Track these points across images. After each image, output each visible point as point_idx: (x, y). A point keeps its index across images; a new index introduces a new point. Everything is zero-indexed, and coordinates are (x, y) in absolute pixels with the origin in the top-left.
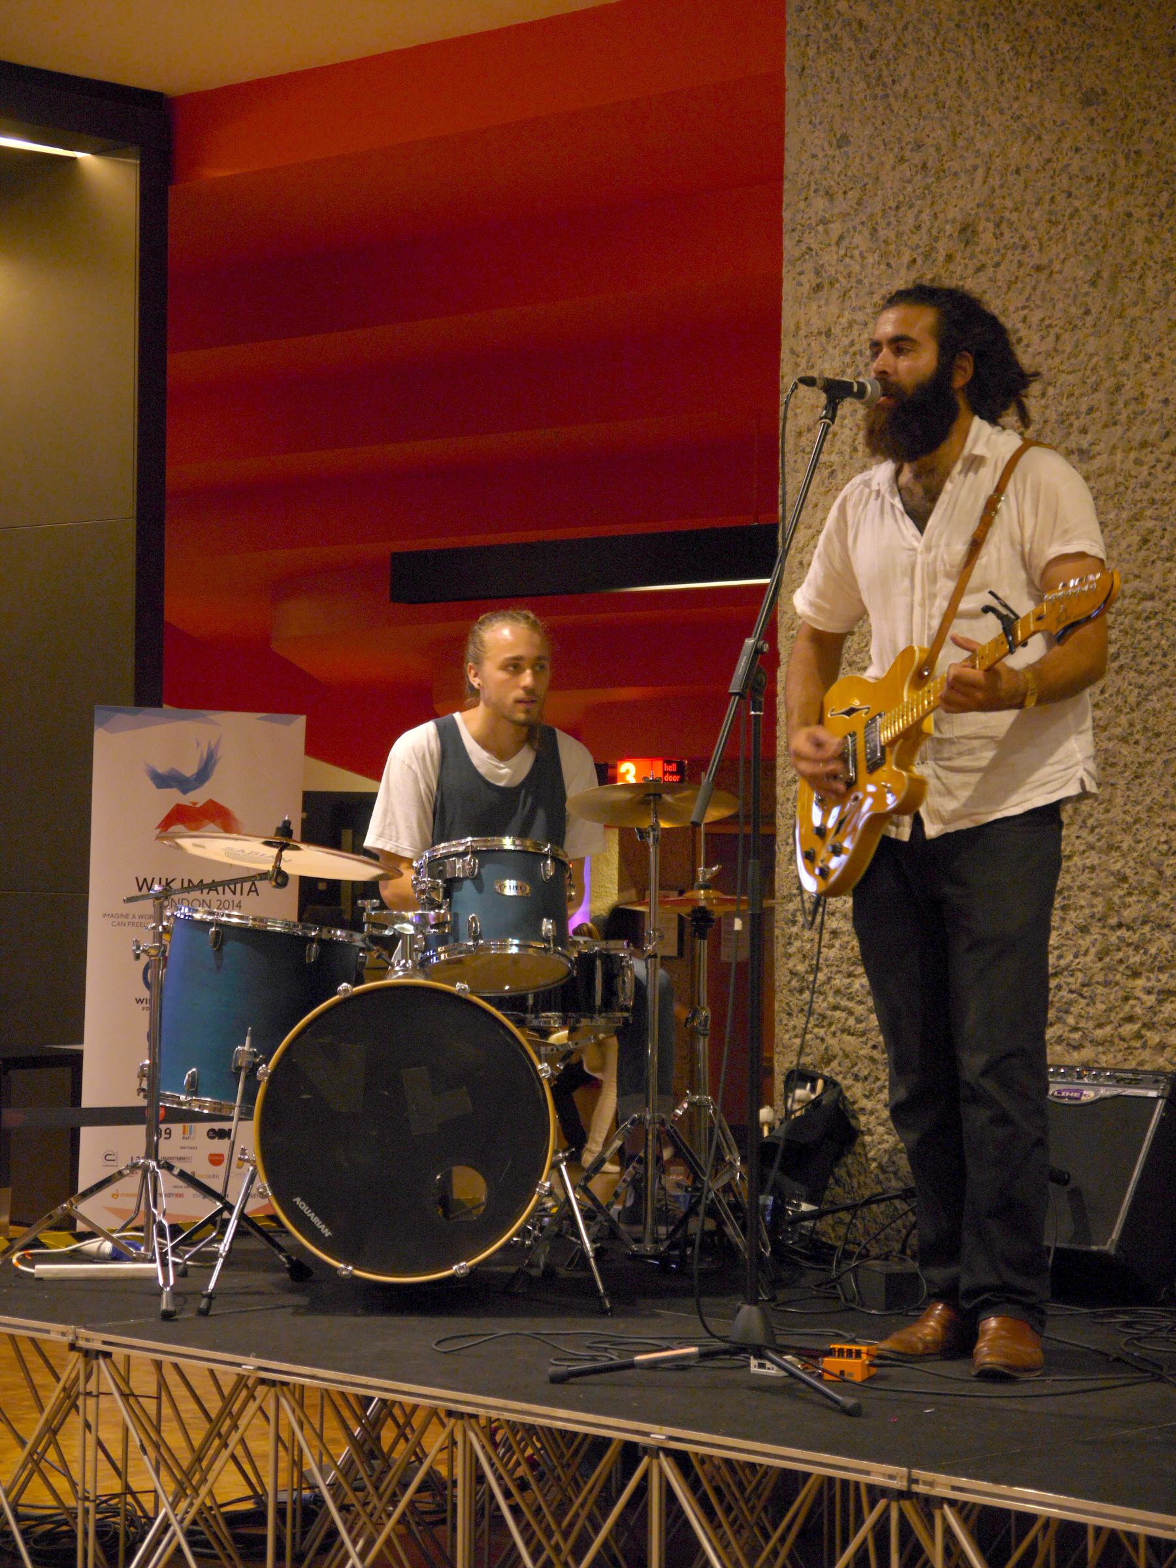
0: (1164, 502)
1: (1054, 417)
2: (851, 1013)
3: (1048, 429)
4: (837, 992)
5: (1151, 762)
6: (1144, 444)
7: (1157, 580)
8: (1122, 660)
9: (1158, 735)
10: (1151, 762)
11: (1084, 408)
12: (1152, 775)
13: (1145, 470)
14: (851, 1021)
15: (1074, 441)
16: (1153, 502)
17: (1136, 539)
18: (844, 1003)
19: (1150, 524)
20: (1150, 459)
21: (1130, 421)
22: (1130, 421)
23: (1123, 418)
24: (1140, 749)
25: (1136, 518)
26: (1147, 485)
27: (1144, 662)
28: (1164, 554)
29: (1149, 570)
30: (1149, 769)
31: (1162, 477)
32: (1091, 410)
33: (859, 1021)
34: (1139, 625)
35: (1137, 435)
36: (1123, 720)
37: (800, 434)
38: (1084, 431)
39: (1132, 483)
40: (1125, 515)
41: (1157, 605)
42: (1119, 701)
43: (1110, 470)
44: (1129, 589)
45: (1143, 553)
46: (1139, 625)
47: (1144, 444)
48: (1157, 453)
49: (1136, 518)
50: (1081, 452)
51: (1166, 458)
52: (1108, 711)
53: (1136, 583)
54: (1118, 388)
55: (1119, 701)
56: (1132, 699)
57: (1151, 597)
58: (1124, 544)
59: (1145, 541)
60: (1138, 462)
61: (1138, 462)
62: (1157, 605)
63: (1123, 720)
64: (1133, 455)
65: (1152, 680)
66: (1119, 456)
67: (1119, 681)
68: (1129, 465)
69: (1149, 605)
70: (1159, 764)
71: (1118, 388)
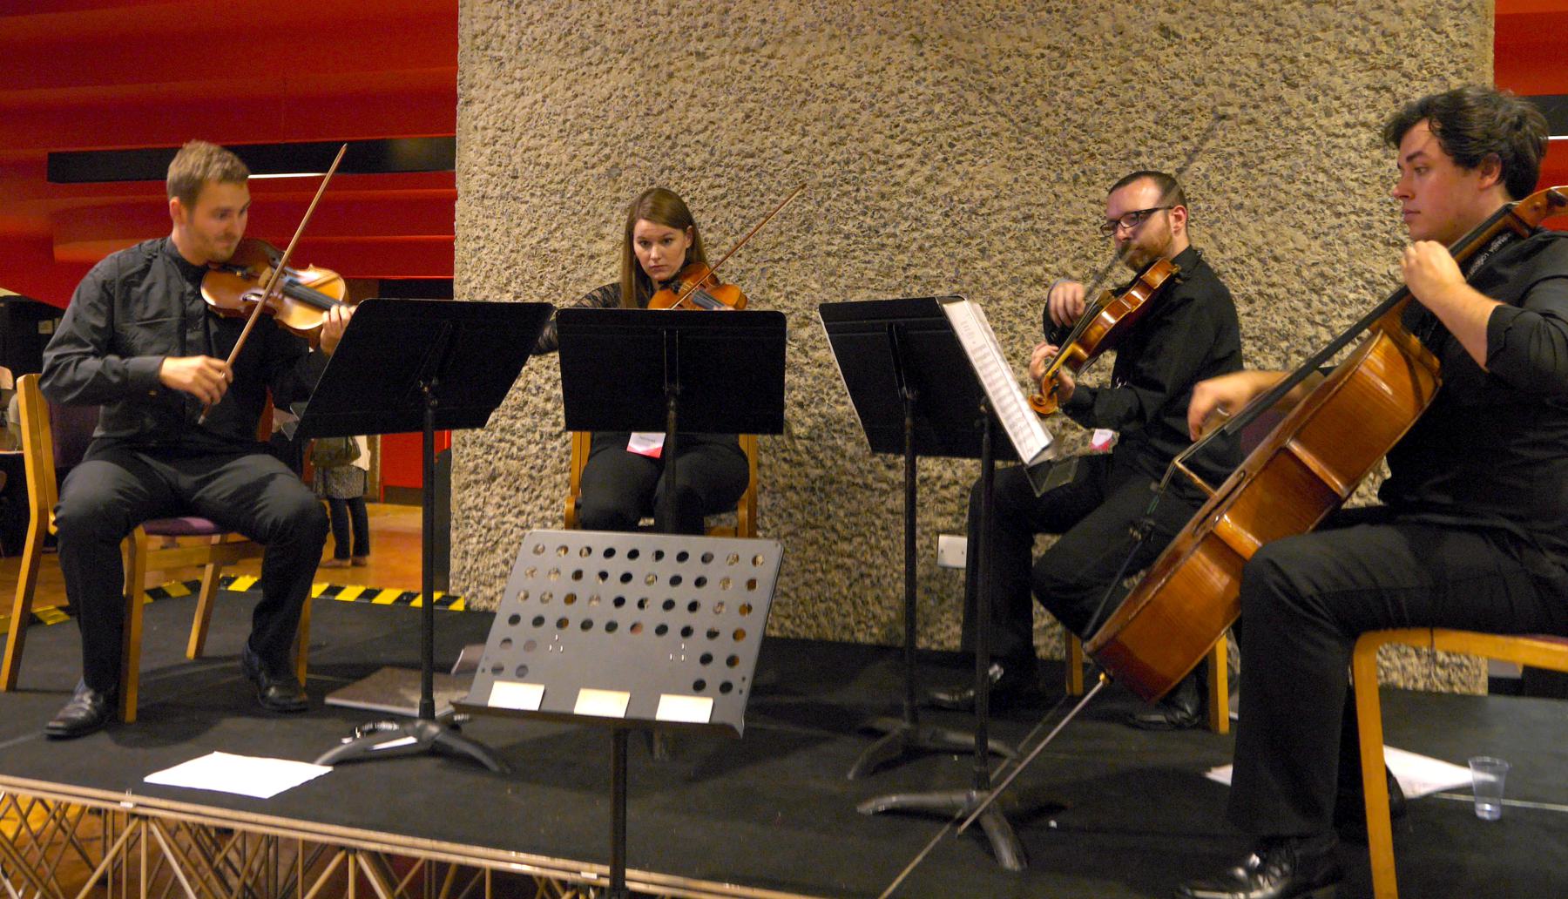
0: (763, 90)
1: (677, 30)
2: (513, 444)
3: (672, 38)
4: (503, 430)
5: (751, 270)
6: (747, 50)
7: (756, 143)
8: (729, 198)
9: (757, 251)
10: (751, 270)
11: (700, 24)
12: (752, 278)
13: (747, 68)
14: (514, 450)
15: (692, 47)
16: (754, 90)
17: (741, 115)
18: (508, 437)
19: (751, 105)
20: (752, 60)
21: (737, 34)
22: (737, 34)
23: (731, 31)
24: (742, 260)
25: (741, 100)
26: (750, 78)
27: (747, 200)
28: (763, 126)
29: (750, 137)
30: (749, 275)
31: (760, 73)
32: (706, 26)
33: (520, 449)
34: (742, 174)
35: (742, 43)
36: (730, 240)
37: (476, 36)
38: (701, 39)
39: (738, 76)
40: (732, 98)
41: (757, 161)
42: (727, 227)
43: (721, 67)
44: (735, 149)
45: (746, 125)
46: (742, 174)
47: (747, 50)
48: (757, 56)
49: (741, 100)
50: (698, 54)
51: (764, 60)
52: (719, 234)
53: (740, 145)
54: (727, 11)
55: (727, 227)
56: (737, 226)
57: (752, 156)
58: (731, 119)
59: (748, 116)
60: (742, 62)
61: (742, 62)
62: (757, 161)
63: (730, 240)
64: (738, 57)
65: (752, 213)
66: (727, 57)
67: (726, 214)
68: (735, 63)
69: (750, 161)
70: (757, 271)
71: (727, 11)
